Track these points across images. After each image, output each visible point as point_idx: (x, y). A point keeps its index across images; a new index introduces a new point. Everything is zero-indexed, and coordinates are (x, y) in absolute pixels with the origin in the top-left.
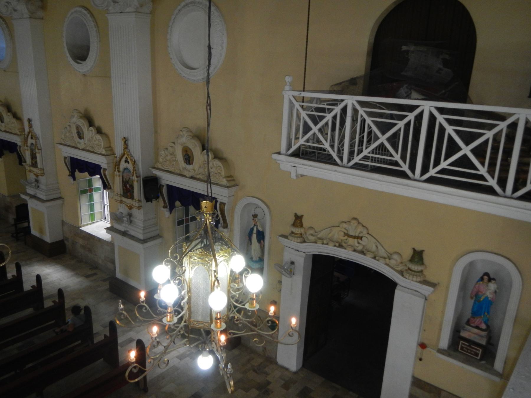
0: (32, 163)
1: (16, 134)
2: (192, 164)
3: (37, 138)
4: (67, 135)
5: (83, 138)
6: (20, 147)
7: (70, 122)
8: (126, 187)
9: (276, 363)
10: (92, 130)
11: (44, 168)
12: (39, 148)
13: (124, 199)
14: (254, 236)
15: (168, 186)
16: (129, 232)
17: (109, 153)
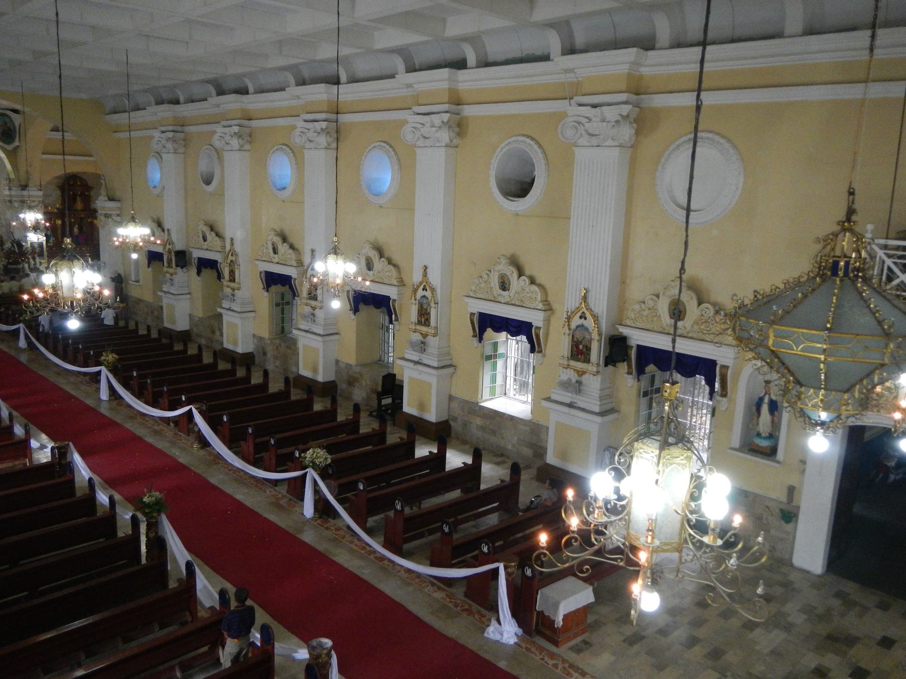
0: (418, 321)
1: (395, 286)
2: (683, 320)
3: (433, 290)
4: (482, 285)
5: (509, 290)
6: (394, 301)
7: (490, 271)
8: (577, 347)
9: (792, 565)
10: (524, 280)
12: (436, 302)
13: (573, 363)
14: (765, 408)
15: (639, 347)
16: (577, 403)
17: (547, 307)
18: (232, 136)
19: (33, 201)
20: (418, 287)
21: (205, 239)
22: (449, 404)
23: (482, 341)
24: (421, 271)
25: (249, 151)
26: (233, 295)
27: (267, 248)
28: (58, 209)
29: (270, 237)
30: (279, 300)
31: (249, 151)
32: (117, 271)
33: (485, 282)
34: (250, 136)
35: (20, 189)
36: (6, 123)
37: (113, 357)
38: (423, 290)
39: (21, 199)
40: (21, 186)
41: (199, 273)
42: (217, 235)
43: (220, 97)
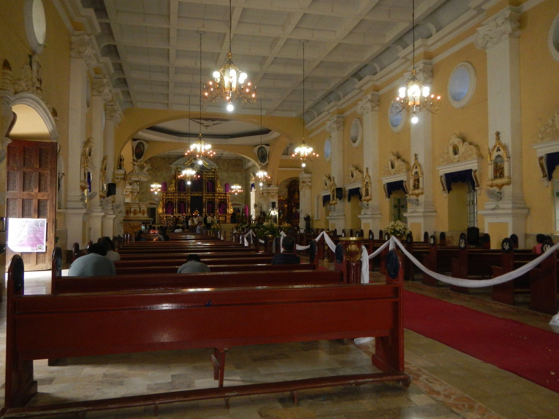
3: (505, 147)
6: (475, 171)
11: (511, 176)
18: (367, 102)
19: (273, 193)
20: (493, 150)
21: (352, 176)
22: (525, 242)
23: (552, 180)
24: (495, 136)
25: (378, 111)
26: (368, 205)
27: (388, 167)
28: (286, 198)
29: (389, 158)
30: (396, 203)
31: (378, 111)
32: (307, 214)
33: (550, 127)
34: (379, 101)
35: (267, 186)
36: (263, 152)
37: (288, 225)
38: (497, 151)
39: (268, 191)
40: (268, 184)
41: (349, 200)
42: (361, 171)
43: (361, 81)
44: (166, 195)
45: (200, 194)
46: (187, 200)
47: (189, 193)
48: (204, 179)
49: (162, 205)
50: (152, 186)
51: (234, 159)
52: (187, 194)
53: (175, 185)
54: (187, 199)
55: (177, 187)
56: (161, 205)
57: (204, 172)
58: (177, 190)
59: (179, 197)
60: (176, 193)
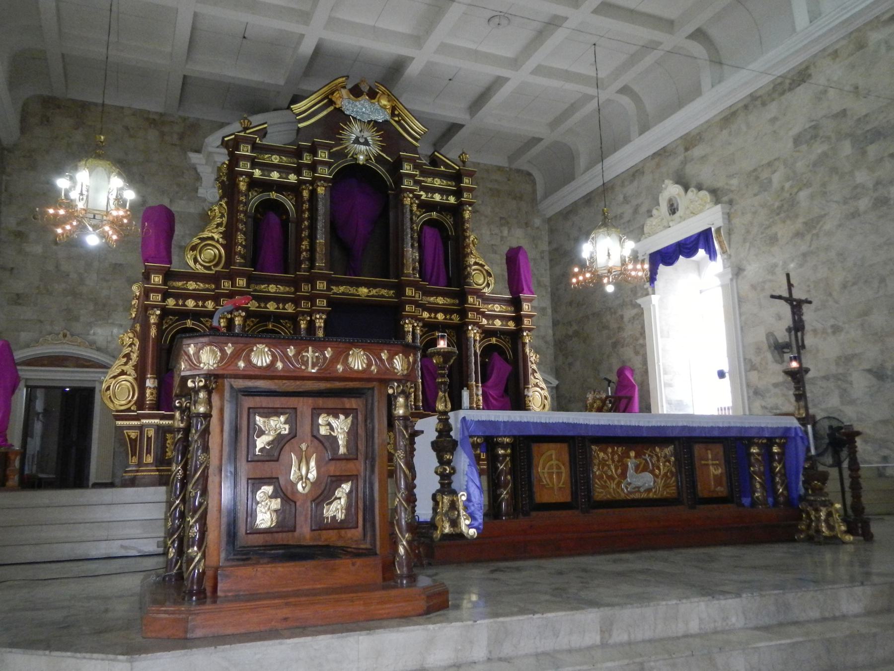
44: (165, 282)
45: (384, 292)
46: (303, 325)
47: (322, 277)
48: (407, 201)
49: (134, 356)
50: (62, 183)
51: (500, 169)
52: (306, 288)
53: (229, 235)
54: (303, 313)
55: (240, 238)
56: (128, 356)
57: (407, 169)
58: (243, 257)
59: (253, 305)
60: (231, 277)
